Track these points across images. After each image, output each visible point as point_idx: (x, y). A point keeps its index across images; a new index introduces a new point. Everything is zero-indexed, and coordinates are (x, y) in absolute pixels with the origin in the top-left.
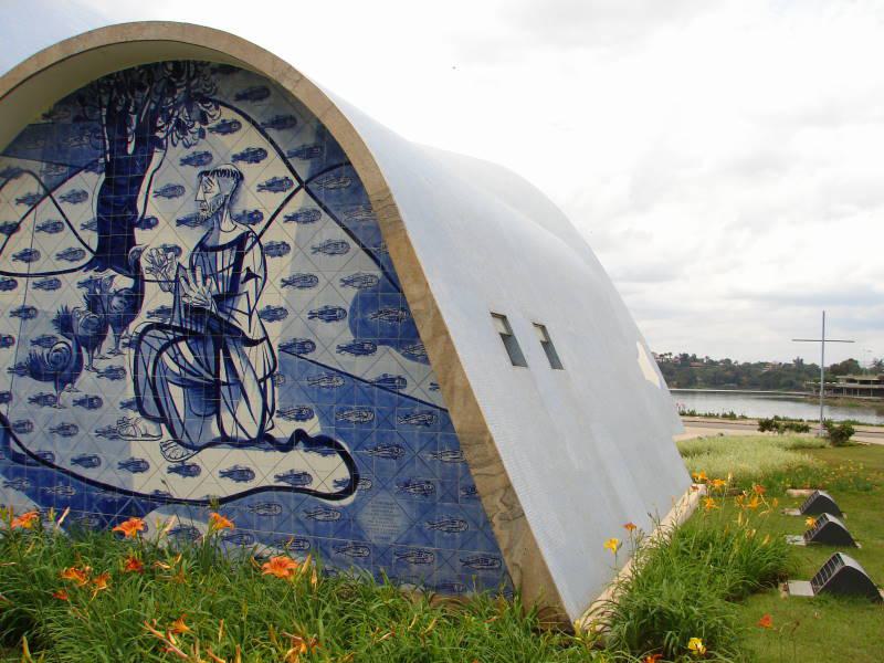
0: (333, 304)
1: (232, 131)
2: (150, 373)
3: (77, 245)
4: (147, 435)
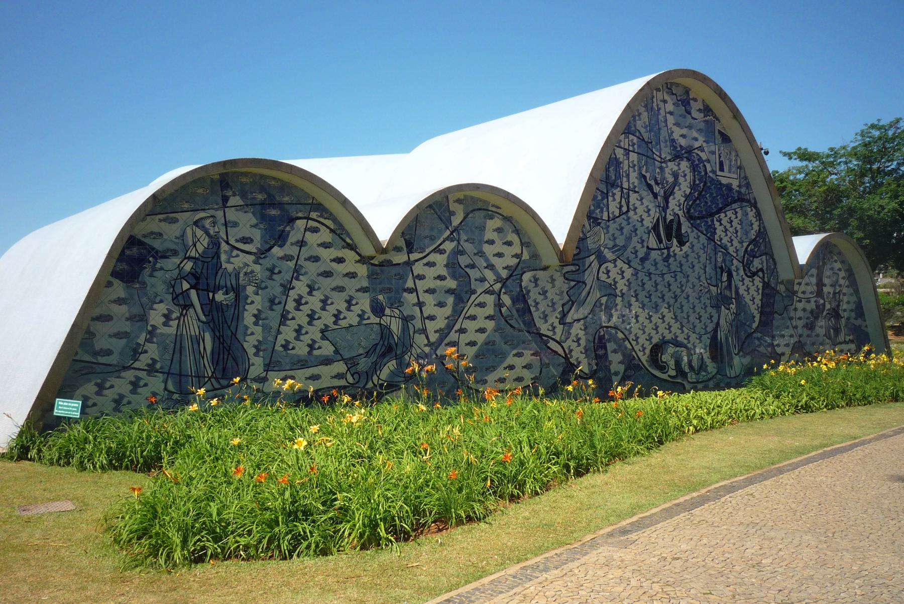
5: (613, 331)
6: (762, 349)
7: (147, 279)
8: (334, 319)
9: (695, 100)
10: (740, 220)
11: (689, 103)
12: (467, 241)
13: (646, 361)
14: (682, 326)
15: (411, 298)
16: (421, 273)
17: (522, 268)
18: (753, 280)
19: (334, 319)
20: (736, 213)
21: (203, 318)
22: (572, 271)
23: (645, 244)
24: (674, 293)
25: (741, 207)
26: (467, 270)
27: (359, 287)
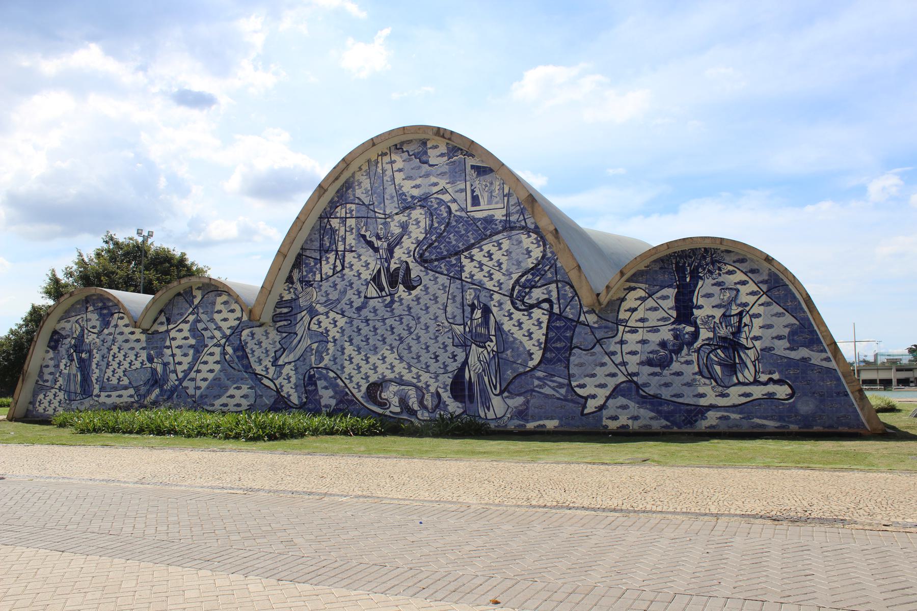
0: (781, 334)
1: (733, 274)
2: (705, 361)
3: (666, 315)
4: (705, 384)
5: (325, 371)
6: (547, 391)
7: (60, 349)
9: (436, 147)
10: (507, 251)
11: (426, 153)
13: (362, 397)
14: (409, 367)
15: (168, 352)
16: (174, 336)
18: (531, 313)
19: (129, 365)
20: (499, 245)
21: (78, 366)
22: (285, 325)
23: (362, 295)
24: (399, 335)
25: (510, 238)
26: (203, 332)
27: (141, 347)
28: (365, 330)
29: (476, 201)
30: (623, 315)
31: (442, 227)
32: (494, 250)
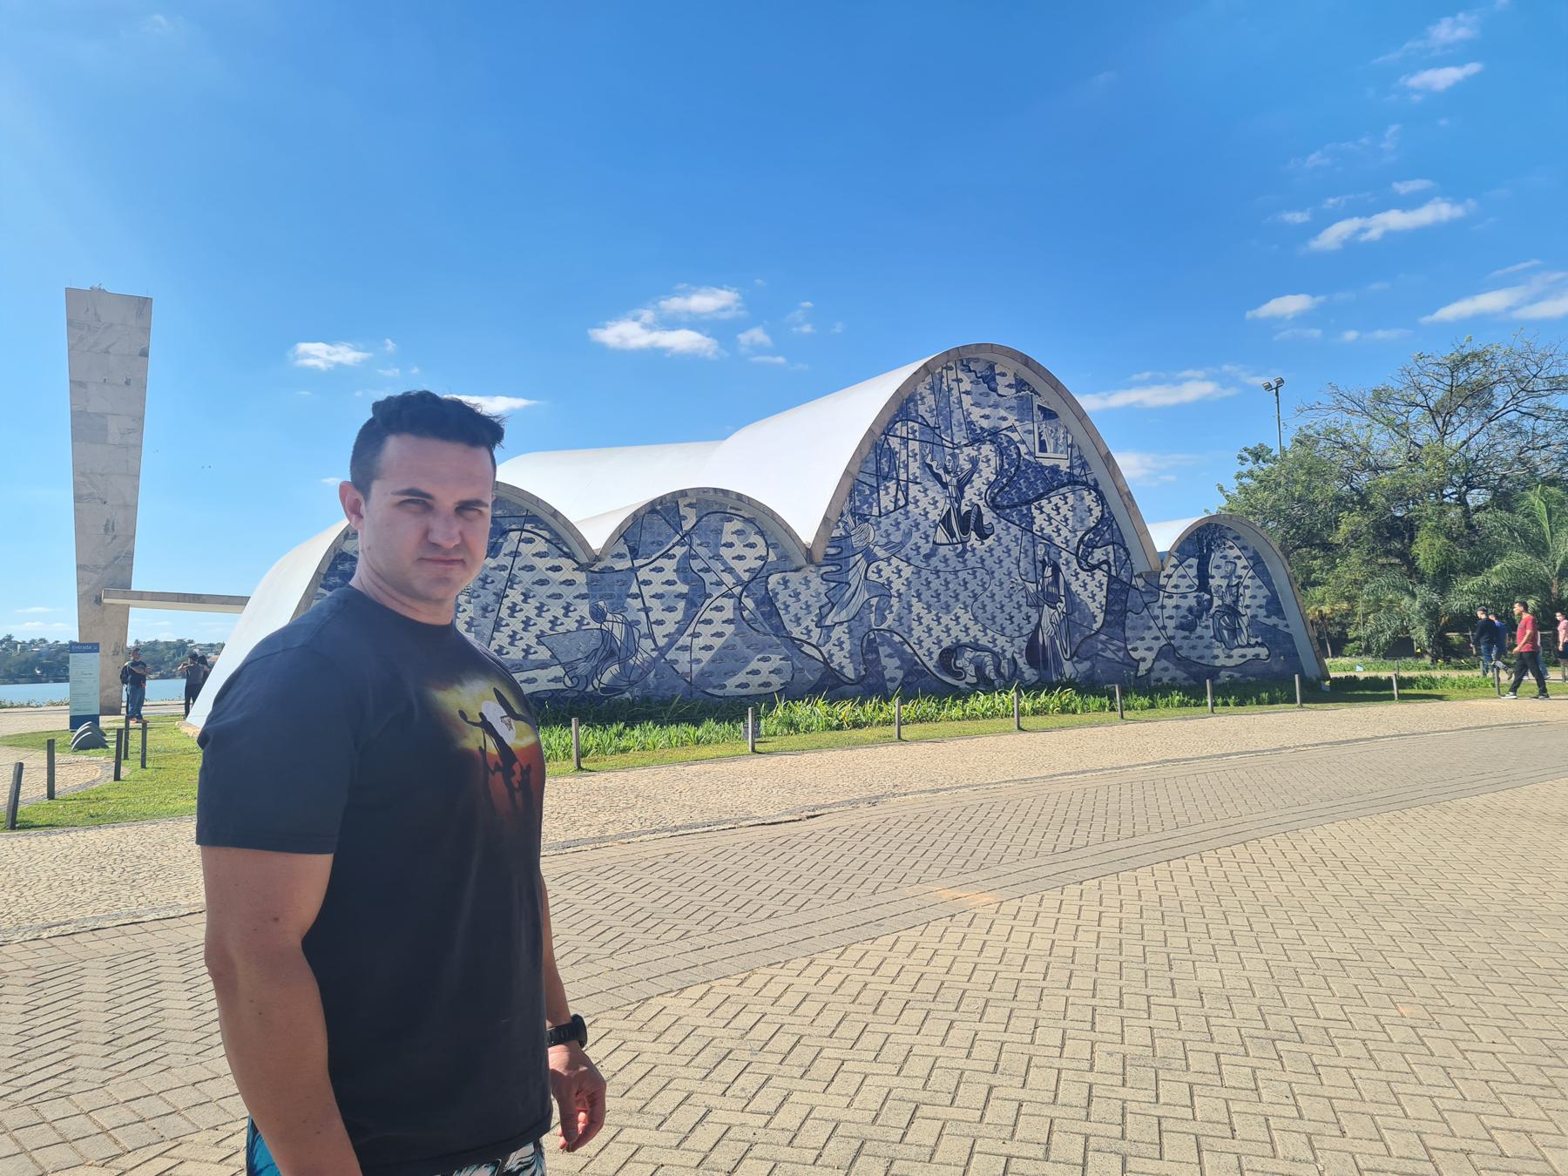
5: (888, 635)
6: (1109, 654)
8: (550, 625)
9: (1004, 375)
11: (995, 380)
12: (700, 545)
15: (637, 603)
17: (768, 571)
19: (550, 625)
20: (1066, 498)
22: (832, 572)
23: (931, 540)
24: (973, 591)
25: (1074, 492)
26: (700, 574)
27: (577, 593)
28: (936, 584)
29: (1043, 448)
30: (1163, 581)
31: (1013, 470)
32: (1061, 503)
